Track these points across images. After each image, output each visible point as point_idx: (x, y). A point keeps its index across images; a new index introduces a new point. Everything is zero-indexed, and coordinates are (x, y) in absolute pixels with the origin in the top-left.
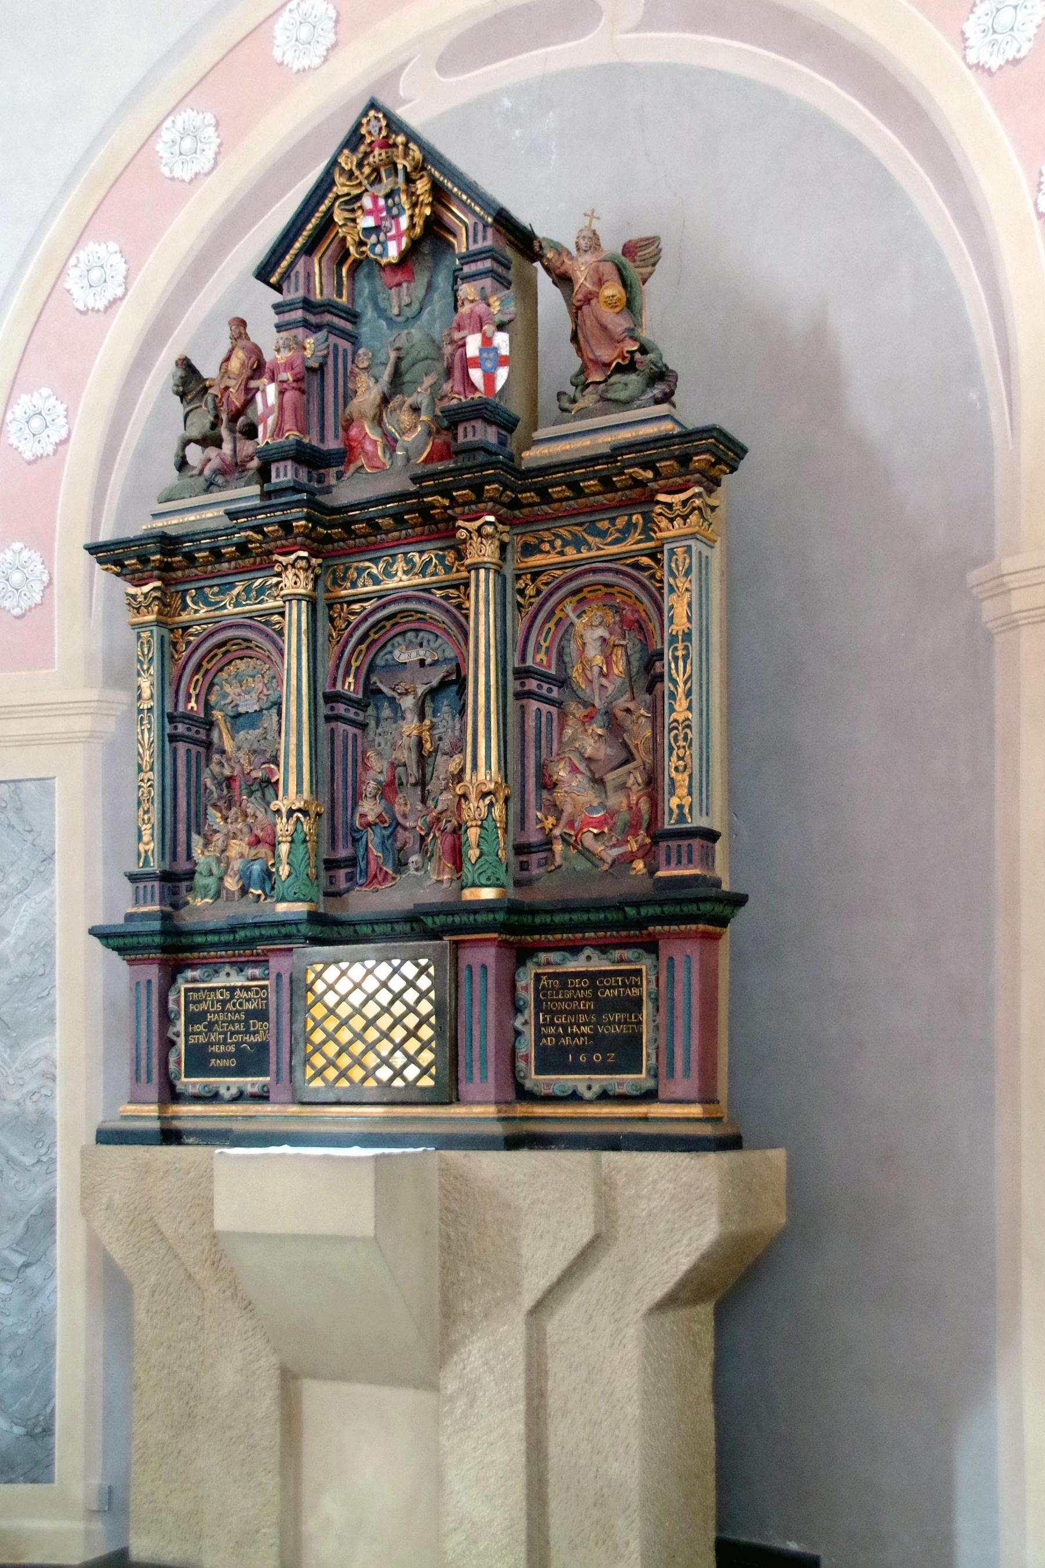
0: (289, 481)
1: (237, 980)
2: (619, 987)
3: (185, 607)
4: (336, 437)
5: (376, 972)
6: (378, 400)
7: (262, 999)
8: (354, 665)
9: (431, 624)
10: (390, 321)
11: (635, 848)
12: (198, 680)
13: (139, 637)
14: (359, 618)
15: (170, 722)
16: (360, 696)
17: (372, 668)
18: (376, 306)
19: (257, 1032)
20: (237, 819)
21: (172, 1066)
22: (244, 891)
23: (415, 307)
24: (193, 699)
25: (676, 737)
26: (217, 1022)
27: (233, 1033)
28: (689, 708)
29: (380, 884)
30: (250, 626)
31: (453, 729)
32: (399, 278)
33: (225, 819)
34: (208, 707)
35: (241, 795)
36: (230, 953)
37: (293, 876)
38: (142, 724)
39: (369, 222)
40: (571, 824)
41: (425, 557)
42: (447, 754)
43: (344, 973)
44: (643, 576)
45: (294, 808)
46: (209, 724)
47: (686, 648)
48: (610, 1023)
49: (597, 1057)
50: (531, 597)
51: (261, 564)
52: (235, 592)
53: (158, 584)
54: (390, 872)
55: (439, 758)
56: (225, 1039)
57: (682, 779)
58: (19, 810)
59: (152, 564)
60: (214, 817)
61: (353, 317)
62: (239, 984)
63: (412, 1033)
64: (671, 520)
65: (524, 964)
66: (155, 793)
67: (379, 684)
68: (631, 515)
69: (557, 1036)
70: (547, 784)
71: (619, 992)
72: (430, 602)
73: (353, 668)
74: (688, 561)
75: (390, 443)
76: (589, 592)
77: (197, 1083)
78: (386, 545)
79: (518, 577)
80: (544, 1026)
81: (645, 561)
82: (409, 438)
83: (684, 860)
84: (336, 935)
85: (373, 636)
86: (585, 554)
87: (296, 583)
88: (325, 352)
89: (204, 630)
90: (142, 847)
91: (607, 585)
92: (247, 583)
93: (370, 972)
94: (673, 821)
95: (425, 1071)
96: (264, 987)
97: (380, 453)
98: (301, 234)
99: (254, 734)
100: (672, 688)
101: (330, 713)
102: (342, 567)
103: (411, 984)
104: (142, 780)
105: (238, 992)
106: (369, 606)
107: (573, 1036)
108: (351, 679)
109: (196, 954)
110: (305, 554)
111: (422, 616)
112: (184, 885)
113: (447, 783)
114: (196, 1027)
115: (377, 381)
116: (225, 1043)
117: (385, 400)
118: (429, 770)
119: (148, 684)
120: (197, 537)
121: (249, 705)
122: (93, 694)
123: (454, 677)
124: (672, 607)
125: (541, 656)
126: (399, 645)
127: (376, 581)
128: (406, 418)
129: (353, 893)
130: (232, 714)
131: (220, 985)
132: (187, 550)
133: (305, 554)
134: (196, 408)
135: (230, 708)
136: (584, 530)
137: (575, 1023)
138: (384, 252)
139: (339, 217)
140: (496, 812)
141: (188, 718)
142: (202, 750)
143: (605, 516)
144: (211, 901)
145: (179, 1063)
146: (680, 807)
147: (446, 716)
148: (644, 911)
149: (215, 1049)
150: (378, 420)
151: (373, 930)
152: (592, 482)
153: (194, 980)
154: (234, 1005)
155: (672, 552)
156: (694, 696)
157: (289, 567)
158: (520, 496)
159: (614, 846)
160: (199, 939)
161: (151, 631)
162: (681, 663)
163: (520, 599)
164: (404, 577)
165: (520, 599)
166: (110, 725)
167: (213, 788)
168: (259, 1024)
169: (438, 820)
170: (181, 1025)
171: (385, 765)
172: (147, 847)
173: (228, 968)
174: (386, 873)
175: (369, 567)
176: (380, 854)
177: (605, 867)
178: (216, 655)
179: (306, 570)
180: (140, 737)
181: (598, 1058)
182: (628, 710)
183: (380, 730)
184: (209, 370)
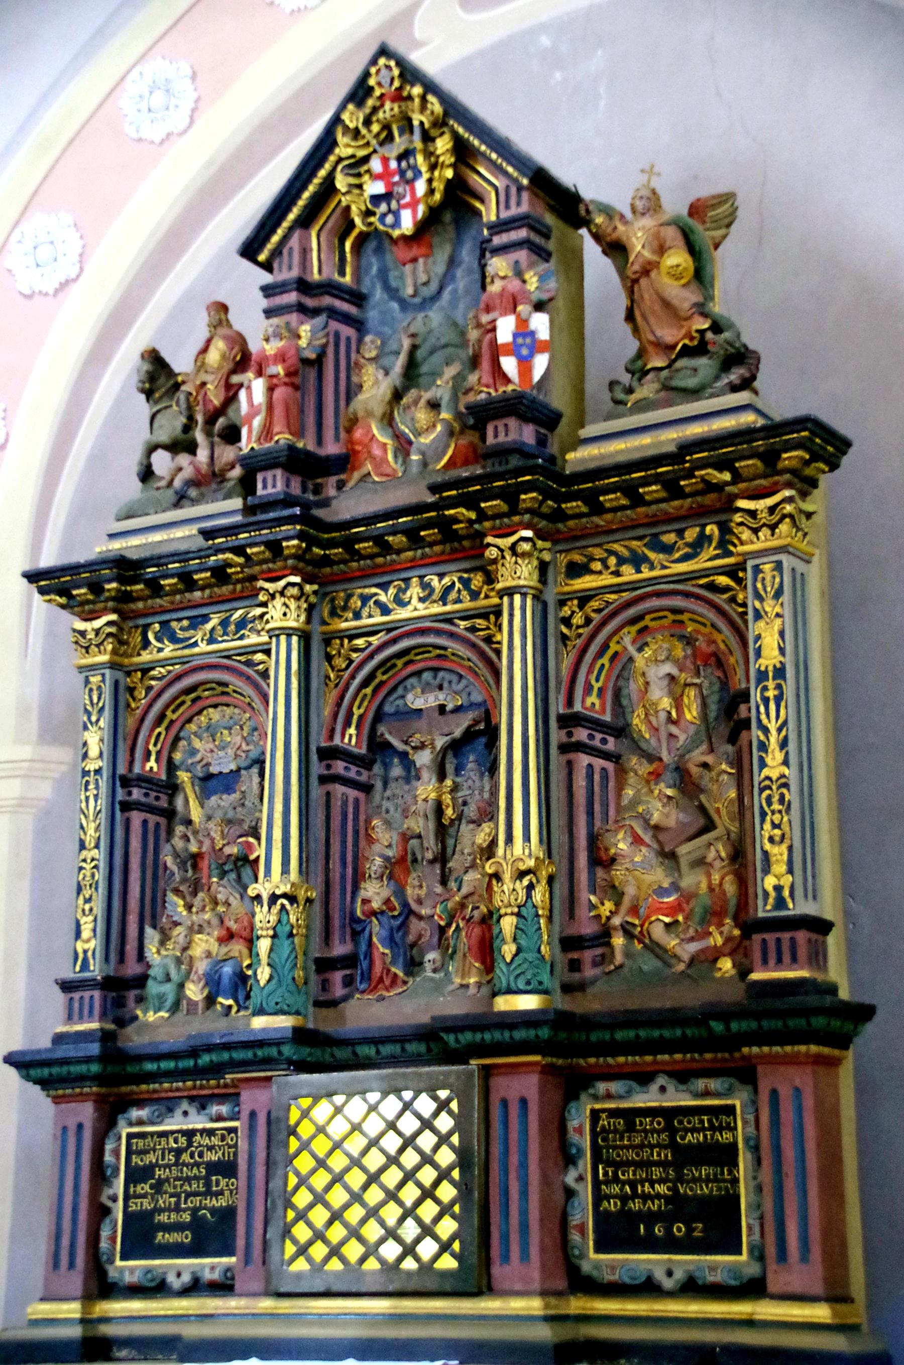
0: (278, 493)
1: (197, 1122)
2: (703, 1129)
3: (146, 644)
4: (337, 438)
5: (381, 1108)
6: (388, 396)
7: (230, 1147)
8: (357, 712)
9: (452, 661)
10: (404, 305)
11: (720, 941)
12: (159, 734)
13: (87, 681)
14: (362, 656)
15: (122, 786)
16: (363, 751)
17: (379, 716)
18: (387, 287)
19: (221, 1193)
20: (204, 906)
21: (104, 1245)
22: (210, 1001)
23: (434, 286)
24: (153, 758)
25: (769, 800)
26: (167, 1180)
27: (188, 1195)
28: (786, 763)
29: (387, 990)
30: (227, 668)
31: (482, 791)
32: (415, 251)
33: (189, 907)
34: (172, 767)
35: (210, 877)
36: (189, 1083)
37: (274, 982)
38: (86, 790)
39: (379, 188)
40: (634, 910)
41: (446, 580)
42: (473, 822)
43: (338, 1110)
44: (720, 599)
45: (278, 892)
46: (172, 788)
47: (779, 687)
48: (695, 1180)
49: (679, 1229)
50: (578, 627)
51: (242, 591)
52: (209, 626)
53: (113, 617)
54: (400, 974)
55: (463, 827)
56: (178, 1203)
57: (778, 853)
59: (107, 594)
60: (176, 905)
61: (358, 298)
62: (199, 1126)
63: (428, 1193)
64: (756, 531)
65: (577, 1098)
66: (100, 876)
67: (388, 736)
68: (703, 526)
69: (624, 1199)
70: (600, 859)
71: (705, 1136)
72: (452, 635)
73: (355, 717)
74: (777, 580)
75: (403, 446)
76: (652, 620)
77: (137, 1267)
78: (398, 567)
79: (562, 603)
80: (607, 1183)
81: (723, 580)
82: (426, 440)
83: (786, 957)
84: (328, 1058)
85: (380, 677)
86: (646, 573)
87: (285, 614)
88: (324, 341)
89: (169, 672)
90: (80, 946)
91: (675, 611)
92: (223, 615)
93: (373, 1108)
94: (769, 907)
95: (445, 1247)
96: (234, 1130)
97: (390, 457)
98: (295, 204)
99: (228, 800)
100: (762, 737)
101: (326, 772)
102: (342, 594)
103: (427, 1124)
104: (84, 860)
105: (198, 1137)
106: (375, 640)
107: (645, 1197)
108: (352, 731)
109: (144, 1087)
110: (297, 579)
111: (442, 652)
112: (132, 994)
113: (475, 859)
114: (139, 1189)
115: (387, 373)
116: (177, 1209)
117: (397, 396)
118: (450, 842)
119: (97, 738)
120: (163, 561)
121: (224, 764)
123: (482, 726)
124: (758, 637)
125: (593, 699)
126: (413, 687)
127: (385, 611)
128: (422, 416)
129: (352, 1002)
130: (200, 775)
131: (174, 1128)
132: (150, 576)
133: (297, 579)
134: (166, 408)
135: (199, 767)
136: (645, 545)
137: (647, 1180)
138: (397, 224)
139: (341, 182)
140: (539, 895)
141: (145, 781)
142: (163, 821)
143: (669, 528)
144: (166, 1015)
145: (113, 1239)
146: (778, 889)
147: (472, 774)
148: (734, 1026)
149: (163, 1218)
150: (388, 420)
151: (378, 1052)
152: (654, 488)
153: (140, 1123)
154: (192, 1156)
155: (757, 570)
156: (792, 746)
157: (278, 595)
158: (563, 506)
159: (692, 939)
160: (150, 1066)
161: (103, 675)
162: (772, 706)
163: (565, 630)
164: (420, 606)
165: (565, 630)
167: (175, 869)
168: (223, 1182)
169: (462, 906)
170: (119, 1185)
171: (396, 838)
172: (86, 946)
173: (185, 1105)
174: (395, 975)
175: (376, 594)
176: (387, 951)
177: (681, 967)
178: (183, 703)
179: (298, 599)
180: (83, 805)
181: (679, 1230)
182: (705, 765)
183: (388, 793)
184: (181, 362)
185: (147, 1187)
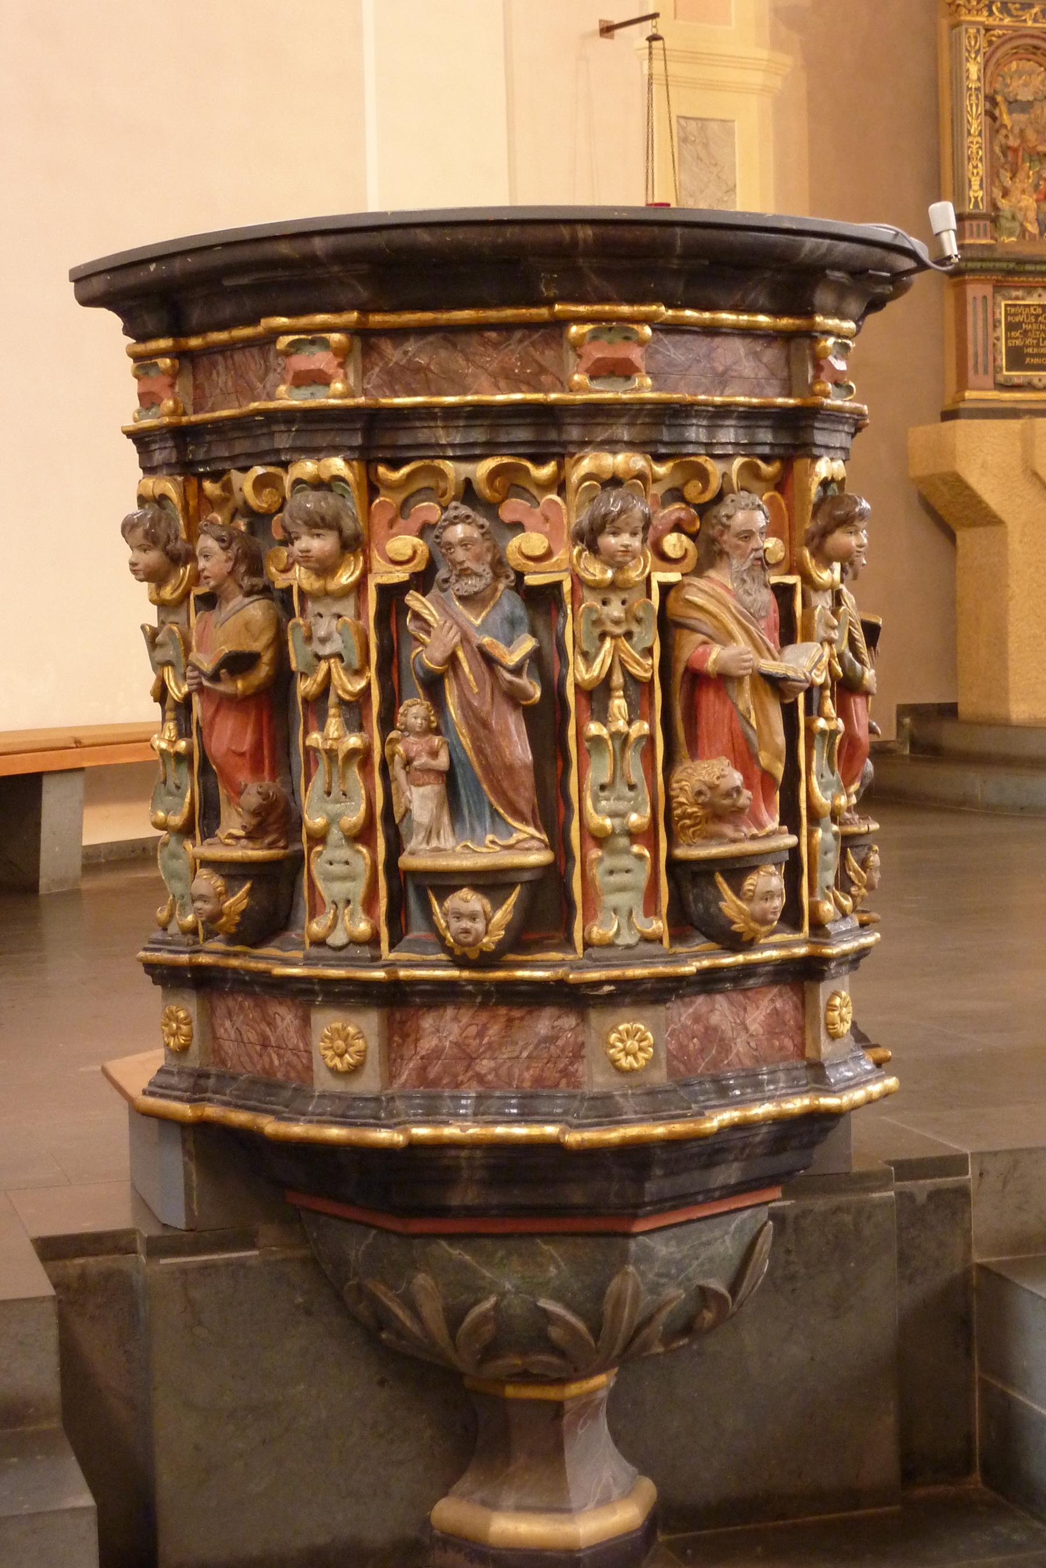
3: (991, 13)
26: (1031, 330)
56: (1038, 344)
58: (706, 145)
121: (1025, 95)
122: (764, 54)
149: (1030, 350)
153: (1017, 298)
166: (777, 82)
167: (1000, 155)
185: (1018, 334)
